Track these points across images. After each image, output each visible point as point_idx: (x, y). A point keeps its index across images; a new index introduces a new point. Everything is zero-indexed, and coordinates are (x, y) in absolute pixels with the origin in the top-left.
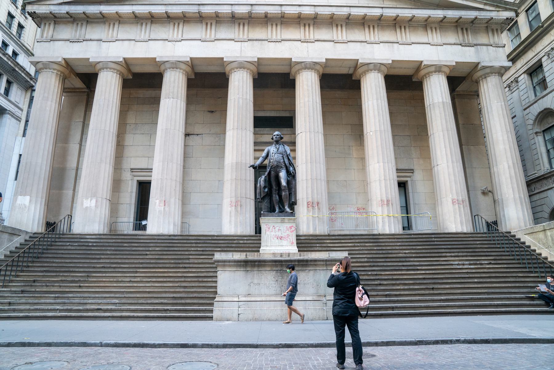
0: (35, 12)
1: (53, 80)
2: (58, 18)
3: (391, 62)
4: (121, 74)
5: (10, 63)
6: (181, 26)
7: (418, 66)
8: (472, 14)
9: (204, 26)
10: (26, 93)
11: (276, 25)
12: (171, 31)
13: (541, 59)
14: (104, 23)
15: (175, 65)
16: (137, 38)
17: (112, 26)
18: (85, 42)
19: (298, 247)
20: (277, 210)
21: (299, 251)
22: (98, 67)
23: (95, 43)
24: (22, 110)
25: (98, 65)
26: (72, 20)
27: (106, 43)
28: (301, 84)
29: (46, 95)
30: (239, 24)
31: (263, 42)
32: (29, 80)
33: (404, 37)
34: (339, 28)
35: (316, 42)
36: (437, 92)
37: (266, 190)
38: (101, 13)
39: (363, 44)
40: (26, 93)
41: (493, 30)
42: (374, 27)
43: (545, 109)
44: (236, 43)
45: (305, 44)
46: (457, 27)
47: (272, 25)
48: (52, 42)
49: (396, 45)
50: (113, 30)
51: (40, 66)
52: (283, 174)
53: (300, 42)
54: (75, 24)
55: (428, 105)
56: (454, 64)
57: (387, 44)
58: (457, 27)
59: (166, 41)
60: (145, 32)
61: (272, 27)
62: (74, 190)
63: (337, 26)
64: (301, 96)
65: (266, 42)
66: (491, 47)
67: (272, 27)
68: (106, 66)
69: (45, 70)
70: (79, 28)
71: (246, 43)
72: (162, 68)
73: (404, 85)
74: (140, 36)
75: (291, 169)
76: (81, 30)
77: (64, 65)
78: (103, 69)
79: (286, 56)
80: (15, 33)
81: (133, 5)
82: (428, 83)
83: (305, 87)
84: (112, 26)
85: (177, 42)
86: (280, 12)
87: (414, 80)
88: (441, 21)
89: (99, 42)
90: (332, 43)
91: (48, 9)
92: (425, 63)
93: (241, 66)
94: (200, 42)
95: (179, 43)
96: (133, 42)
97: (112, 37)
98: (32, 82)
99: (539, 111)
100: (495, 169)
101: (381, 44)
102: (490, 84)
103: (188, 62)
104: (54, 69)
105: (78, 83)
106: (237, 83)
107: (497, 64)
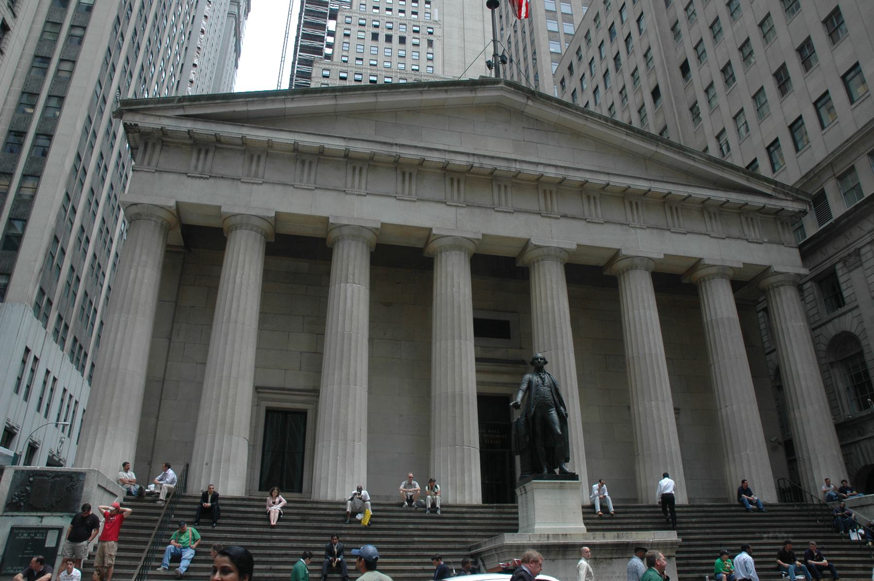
3: (662, 256)
4: (265, 235)
6: (364, 171)
7: (697, 263)
8: (759, 201)
9: (400, 178)
11: (506, 187)
12: (349, 178)
13: (834, 265)
14: (244, 152)
15: (357, 233)
16: (297, 184)
18: (211, 181)
19: (585, 524)
20: (546, 471)
21: (588, 530)
22: (233, 221)
25: (233, 218)
26: (191, 142)
28: (542, 279)
30: (452, 180)
31: (489, 211)
33: (677, 224)
34: (592, 201)
35: (563, 220)
36: (721, 305)
37: (528, 440)
39: (624, 227)
41: (782, 223)
42: (637, 204)
43: (844, 332)
44: (448, 208)
45: (547, 220)
46: (740, 214)
47: (499, 186)
48: (157, 174)
49: (667, 233)
52: (554, 414)
53: (539, 217)
55: (709, 319)
56: (742, 266)
57: (655, 231)
58: (740, 214)
59: (343, 194)
60: (309, 174)
61: (499, 190)
62: (157, 418)
63: (589, 197)
64: (543, 296)
65: (493, 212)
66: (782, 247)
67: (499, 190)
68: (244, 222)
71: (463, 211)
72: (334, 234)
73: (678, 289)
74: (301, 181)
75: (562, 408)
79: (522, 234)
82: (708, 289)
83: (548, 282)
85: (360, 197)
86: (514, 170)
87: (685, 281)
88: (722, 205)
89: (235, 182)
90: (583, 223)
92: (707, 262)
93: (457, 245)
94: (394, 200)
95: (363, 198)
96: (292, 188)
99: (834, 333)
100: (797, 415)
101: (648, 230)
102: (783, 296)
103: (377, 229)
105: (176, 238)
106: (450, 269)
107: (792, 270)
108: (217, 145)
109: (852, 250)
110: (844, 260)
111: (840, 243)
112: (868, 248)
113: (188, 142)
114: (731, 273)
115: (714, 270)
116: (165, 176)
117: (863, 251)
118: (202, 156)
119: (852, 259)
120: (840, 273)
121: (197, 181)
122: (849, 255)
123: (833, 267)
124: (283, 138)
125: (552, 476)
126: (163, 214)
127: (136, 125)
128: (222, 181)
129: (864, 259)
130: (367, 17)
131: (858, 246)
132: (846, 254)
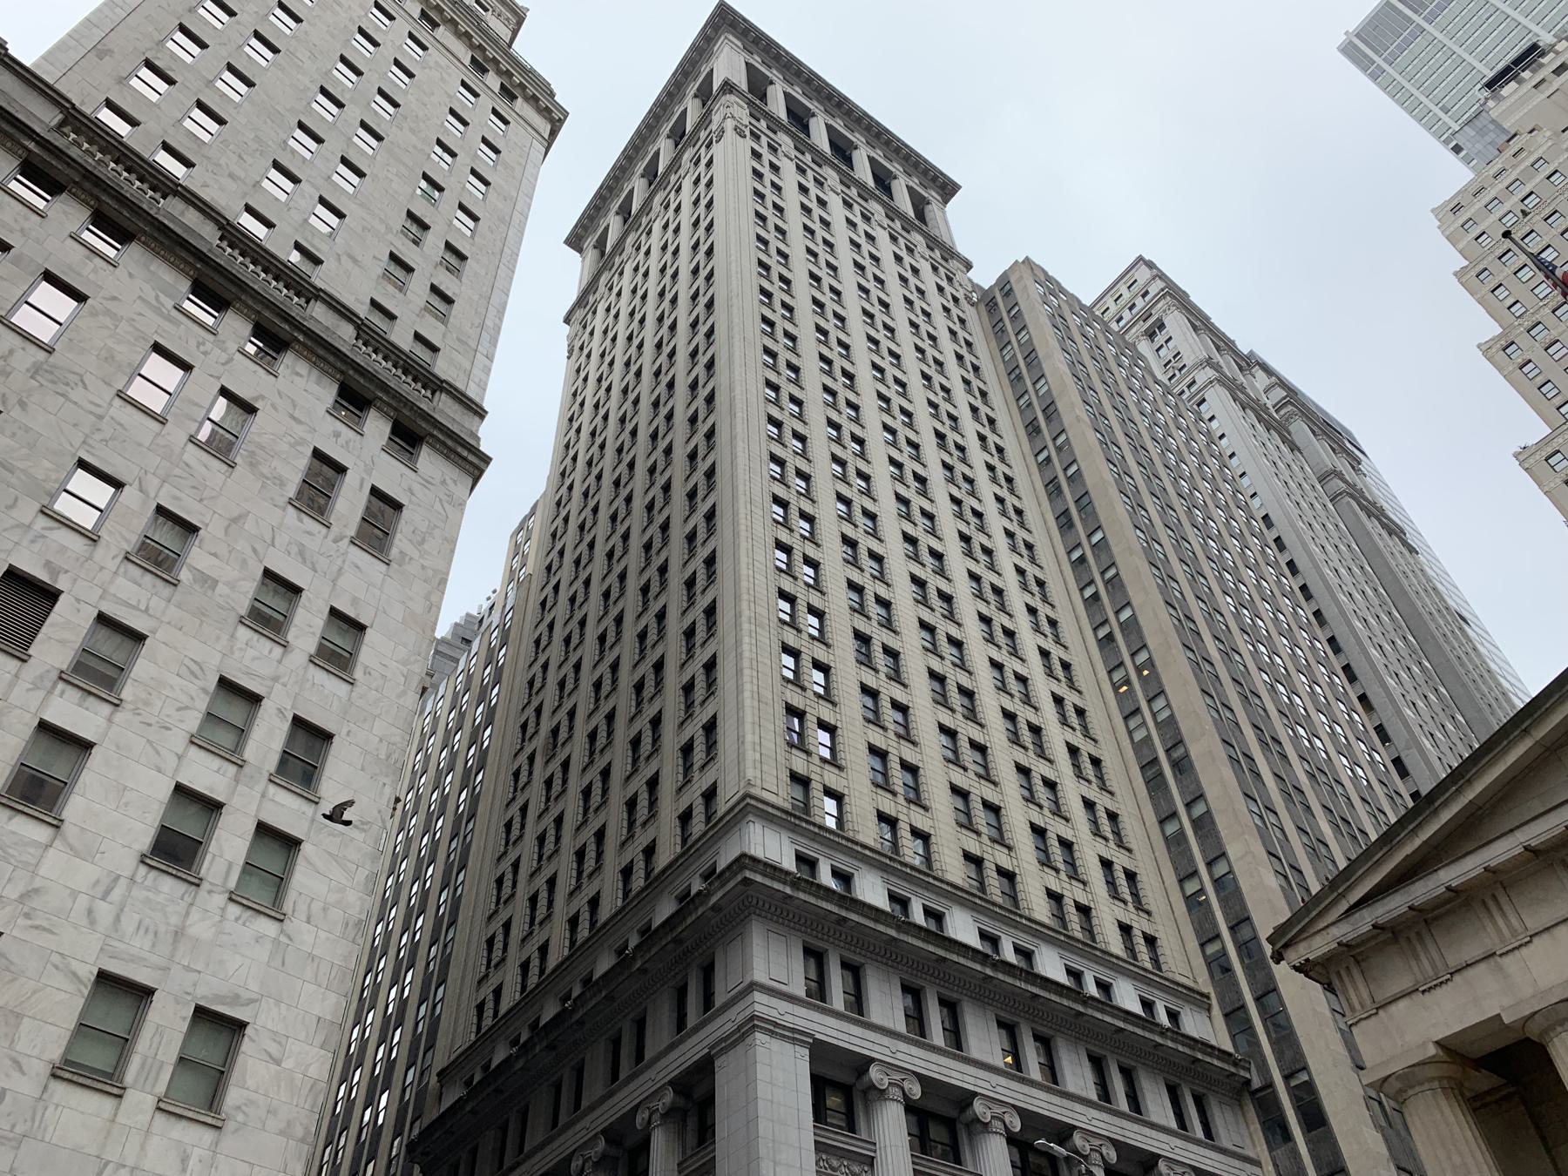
0: (1307, 960)
1: (1447, 1111)
2: (1358, 945)
5: (1180, 1048)
10: (1241, 1106)
17: (1491, 904)
18: (1457, 978)
23: (1482, 966)
24: (1257, 1163)
27: (1510, 957)
29: (1457, 1160)
32: (1233, 1070)
38: (1449, 889)
40: (1241, 1106)
50: (1504, 915)
51: (1395, 1085)
54: (1403, 943)
69: (1411, 1092)
70: (1419, 947)
76: (1426, 951)
77: (1446, 1058)
78: (1552, 1028)
80: (1079, 935)
81: (1511, 831)
84: (1491, 904)
89: (1492, 961)
91: (1330, 938)
97: (1514, 933)
98: (1242, 1073)
104: (1431, 1080)
105: (1483, 1081)
108: (1427, 919)
113: (1382, 938)
116: (1393, 1008)
118: (1419, 947)
121: (1439, 991)
124: (1502, 851)
126: (1431, 1071)
127: (1307, 960)
128: (1471, 972)
130: (1538, 317)
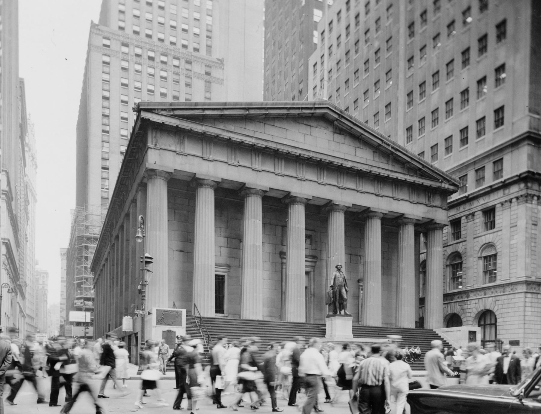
109: (471, 212)
110: (467, 217)
111: (467, 206)
112: (479, 212)
114: (415, 221)
115: (409, 220)
117: (476, 214)
119: (470, 217)
120: (462, 222)
122: (469, 214)
123: (460, 218)
125: (340, 315)
127: (149, 119)
129: (475, 218)
131: (474, 211)
132: (468, 213)
